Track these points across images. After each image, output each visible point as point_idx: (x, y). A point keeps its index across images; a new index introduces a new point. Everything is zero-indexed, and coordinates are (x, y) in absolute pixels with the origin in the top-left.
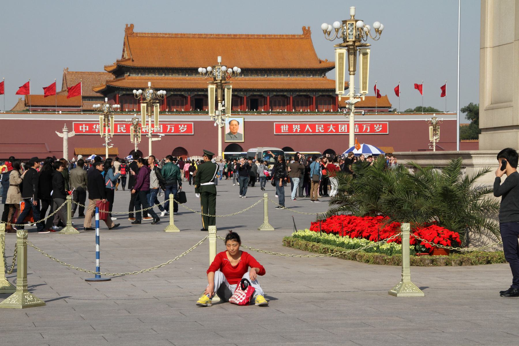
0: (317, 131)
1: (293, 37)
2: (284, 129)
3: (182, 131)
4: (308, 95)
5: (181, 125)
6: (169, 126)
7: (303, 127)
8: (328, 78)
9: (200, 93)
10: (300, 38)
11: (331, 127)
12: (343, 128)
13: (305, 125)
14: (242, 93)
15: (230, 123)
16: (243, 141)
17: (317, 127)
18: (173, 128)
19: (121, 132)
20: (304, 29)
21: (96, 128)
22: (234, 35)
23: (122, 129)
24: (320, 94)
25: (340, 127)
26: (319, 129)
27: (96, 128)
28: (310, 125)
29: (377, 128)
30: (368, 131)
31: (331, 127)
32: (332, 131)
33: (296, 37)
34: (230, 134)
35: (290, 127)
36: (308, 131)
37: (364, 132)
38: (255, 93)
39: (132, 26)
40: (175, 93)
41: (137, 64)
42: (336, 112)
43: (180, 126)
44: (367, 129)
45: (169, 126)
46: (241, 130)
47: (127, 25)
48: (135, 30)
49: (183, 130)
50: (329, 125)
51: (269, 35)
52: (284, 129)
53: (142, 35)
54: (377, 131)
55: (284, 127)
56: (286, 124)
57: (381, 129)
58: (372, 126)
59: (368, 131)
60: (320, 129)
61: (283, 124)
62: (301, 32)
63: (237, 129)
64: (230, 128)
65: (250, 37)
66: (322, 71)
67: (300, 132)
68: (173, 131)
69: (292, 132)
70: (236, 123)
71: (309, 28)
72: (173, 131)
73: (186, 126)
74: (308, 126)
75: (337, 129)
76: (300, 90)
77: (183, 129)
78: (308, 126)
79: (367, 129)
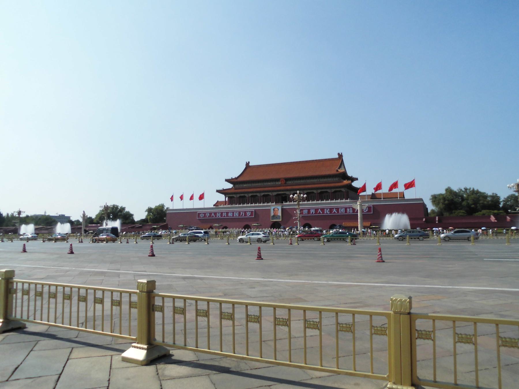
11: (334, 210)
13: (318, 209)
15: (274, 209)
20: (339, 154)
26: (327, 212)
28: (321, 209)
31: (334, 210)
34: (274, 216)
35: (309, 210)
36: (320, 213)
39: (249, 162)
46: (280, 214)
48: (250, 165)
50: (333, 209)
62: (337, 156)
75: (338, 211)
77: (248, 214)
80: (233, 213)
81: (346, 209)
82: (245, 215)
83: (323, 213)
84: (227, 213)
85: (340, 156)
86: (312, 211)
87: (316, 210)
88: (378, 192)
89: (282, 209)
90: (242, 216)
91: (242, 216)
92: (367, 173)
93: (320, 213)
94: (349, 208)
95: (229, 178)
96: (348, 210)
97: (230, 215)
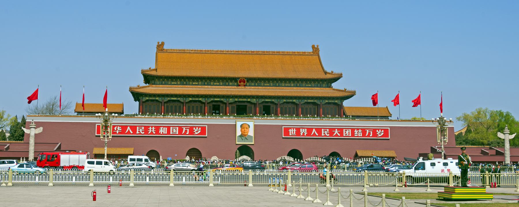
0: (323, 135)
1: (304, 54)
2: (292, 132)
3: (196, 133)
4: (315, 103)
5: (196, 127)
6: (184, 128)
7: (310, 130)
8: (334, 88)
9: (216, 99)
10: (309, 54)
11: (336, 131)
12: (347, 132)
14: (254, 100)
15: (241, 126)
16: (253, 143)
17: (323, 131)
18: (188, 130)
19: (140, 134)
20: (313, 47)
21: (117, 130)
22: (252, 52)
23: (141, 131)
24: (327, 101)
25: (344, 131)
27: (117, 130)
29: (379, 133)
30: (371, 135)
31: (336, 131)
32: (337, 135)
33: (307, 54)
34: (241, 136)
35: (298, 131)
36: (314, 135)
37: (367, 137)
38: (267, 100)
39: (163, 44)
40: (194, 99)
41: (160, 73)
42: (340, 116)
43: (194, 129)
44: (369, 133)
45: (184, 128)
46: (251, 132)
47: (158, 43)
49: (197, 132)
50: (334, 129)
51: (283, 52)
52: (292, 132)
53: (171, 51)
54: (379, 135)
55: (292, 131)
56: (293, 128)
57: (382, 134)
58: (374, 131)
59: (371, 135)
60: (326, 133)
61: (291, 128)
62: (311, 50)
63: (248, 132)
64: (241, 131)
65: (266, 53)
66: (329, 82)
67: (307, 135)
68: (187, 133)
69: (299, 135)
70: (248, 126)
71: (318, 46)
72: (187, 133)
73: (200, 129)
74: (314, 130)
75: (341, 133)
76: (308, 98)
77: (197, 131)
78: (314, 130)
79: (369, 133)
80: (169, 128)
81: (353, 130)
82: (192, 132)
83: (320, 134)
84: (157, 129)
85: (316, 50)
86: (302, 131)
87: (310, 130)
88: (377, 106)
89: (255, 126)
90: (185, 134)
91: (185, 134)
92: (359, 80)
93: (314, 135)
94: (358, 129)
95: (146, 68)
96: (356, 131)
97: (163, 131)
